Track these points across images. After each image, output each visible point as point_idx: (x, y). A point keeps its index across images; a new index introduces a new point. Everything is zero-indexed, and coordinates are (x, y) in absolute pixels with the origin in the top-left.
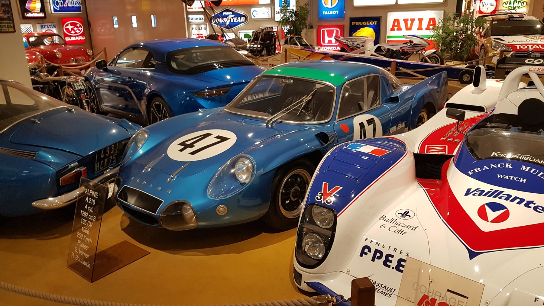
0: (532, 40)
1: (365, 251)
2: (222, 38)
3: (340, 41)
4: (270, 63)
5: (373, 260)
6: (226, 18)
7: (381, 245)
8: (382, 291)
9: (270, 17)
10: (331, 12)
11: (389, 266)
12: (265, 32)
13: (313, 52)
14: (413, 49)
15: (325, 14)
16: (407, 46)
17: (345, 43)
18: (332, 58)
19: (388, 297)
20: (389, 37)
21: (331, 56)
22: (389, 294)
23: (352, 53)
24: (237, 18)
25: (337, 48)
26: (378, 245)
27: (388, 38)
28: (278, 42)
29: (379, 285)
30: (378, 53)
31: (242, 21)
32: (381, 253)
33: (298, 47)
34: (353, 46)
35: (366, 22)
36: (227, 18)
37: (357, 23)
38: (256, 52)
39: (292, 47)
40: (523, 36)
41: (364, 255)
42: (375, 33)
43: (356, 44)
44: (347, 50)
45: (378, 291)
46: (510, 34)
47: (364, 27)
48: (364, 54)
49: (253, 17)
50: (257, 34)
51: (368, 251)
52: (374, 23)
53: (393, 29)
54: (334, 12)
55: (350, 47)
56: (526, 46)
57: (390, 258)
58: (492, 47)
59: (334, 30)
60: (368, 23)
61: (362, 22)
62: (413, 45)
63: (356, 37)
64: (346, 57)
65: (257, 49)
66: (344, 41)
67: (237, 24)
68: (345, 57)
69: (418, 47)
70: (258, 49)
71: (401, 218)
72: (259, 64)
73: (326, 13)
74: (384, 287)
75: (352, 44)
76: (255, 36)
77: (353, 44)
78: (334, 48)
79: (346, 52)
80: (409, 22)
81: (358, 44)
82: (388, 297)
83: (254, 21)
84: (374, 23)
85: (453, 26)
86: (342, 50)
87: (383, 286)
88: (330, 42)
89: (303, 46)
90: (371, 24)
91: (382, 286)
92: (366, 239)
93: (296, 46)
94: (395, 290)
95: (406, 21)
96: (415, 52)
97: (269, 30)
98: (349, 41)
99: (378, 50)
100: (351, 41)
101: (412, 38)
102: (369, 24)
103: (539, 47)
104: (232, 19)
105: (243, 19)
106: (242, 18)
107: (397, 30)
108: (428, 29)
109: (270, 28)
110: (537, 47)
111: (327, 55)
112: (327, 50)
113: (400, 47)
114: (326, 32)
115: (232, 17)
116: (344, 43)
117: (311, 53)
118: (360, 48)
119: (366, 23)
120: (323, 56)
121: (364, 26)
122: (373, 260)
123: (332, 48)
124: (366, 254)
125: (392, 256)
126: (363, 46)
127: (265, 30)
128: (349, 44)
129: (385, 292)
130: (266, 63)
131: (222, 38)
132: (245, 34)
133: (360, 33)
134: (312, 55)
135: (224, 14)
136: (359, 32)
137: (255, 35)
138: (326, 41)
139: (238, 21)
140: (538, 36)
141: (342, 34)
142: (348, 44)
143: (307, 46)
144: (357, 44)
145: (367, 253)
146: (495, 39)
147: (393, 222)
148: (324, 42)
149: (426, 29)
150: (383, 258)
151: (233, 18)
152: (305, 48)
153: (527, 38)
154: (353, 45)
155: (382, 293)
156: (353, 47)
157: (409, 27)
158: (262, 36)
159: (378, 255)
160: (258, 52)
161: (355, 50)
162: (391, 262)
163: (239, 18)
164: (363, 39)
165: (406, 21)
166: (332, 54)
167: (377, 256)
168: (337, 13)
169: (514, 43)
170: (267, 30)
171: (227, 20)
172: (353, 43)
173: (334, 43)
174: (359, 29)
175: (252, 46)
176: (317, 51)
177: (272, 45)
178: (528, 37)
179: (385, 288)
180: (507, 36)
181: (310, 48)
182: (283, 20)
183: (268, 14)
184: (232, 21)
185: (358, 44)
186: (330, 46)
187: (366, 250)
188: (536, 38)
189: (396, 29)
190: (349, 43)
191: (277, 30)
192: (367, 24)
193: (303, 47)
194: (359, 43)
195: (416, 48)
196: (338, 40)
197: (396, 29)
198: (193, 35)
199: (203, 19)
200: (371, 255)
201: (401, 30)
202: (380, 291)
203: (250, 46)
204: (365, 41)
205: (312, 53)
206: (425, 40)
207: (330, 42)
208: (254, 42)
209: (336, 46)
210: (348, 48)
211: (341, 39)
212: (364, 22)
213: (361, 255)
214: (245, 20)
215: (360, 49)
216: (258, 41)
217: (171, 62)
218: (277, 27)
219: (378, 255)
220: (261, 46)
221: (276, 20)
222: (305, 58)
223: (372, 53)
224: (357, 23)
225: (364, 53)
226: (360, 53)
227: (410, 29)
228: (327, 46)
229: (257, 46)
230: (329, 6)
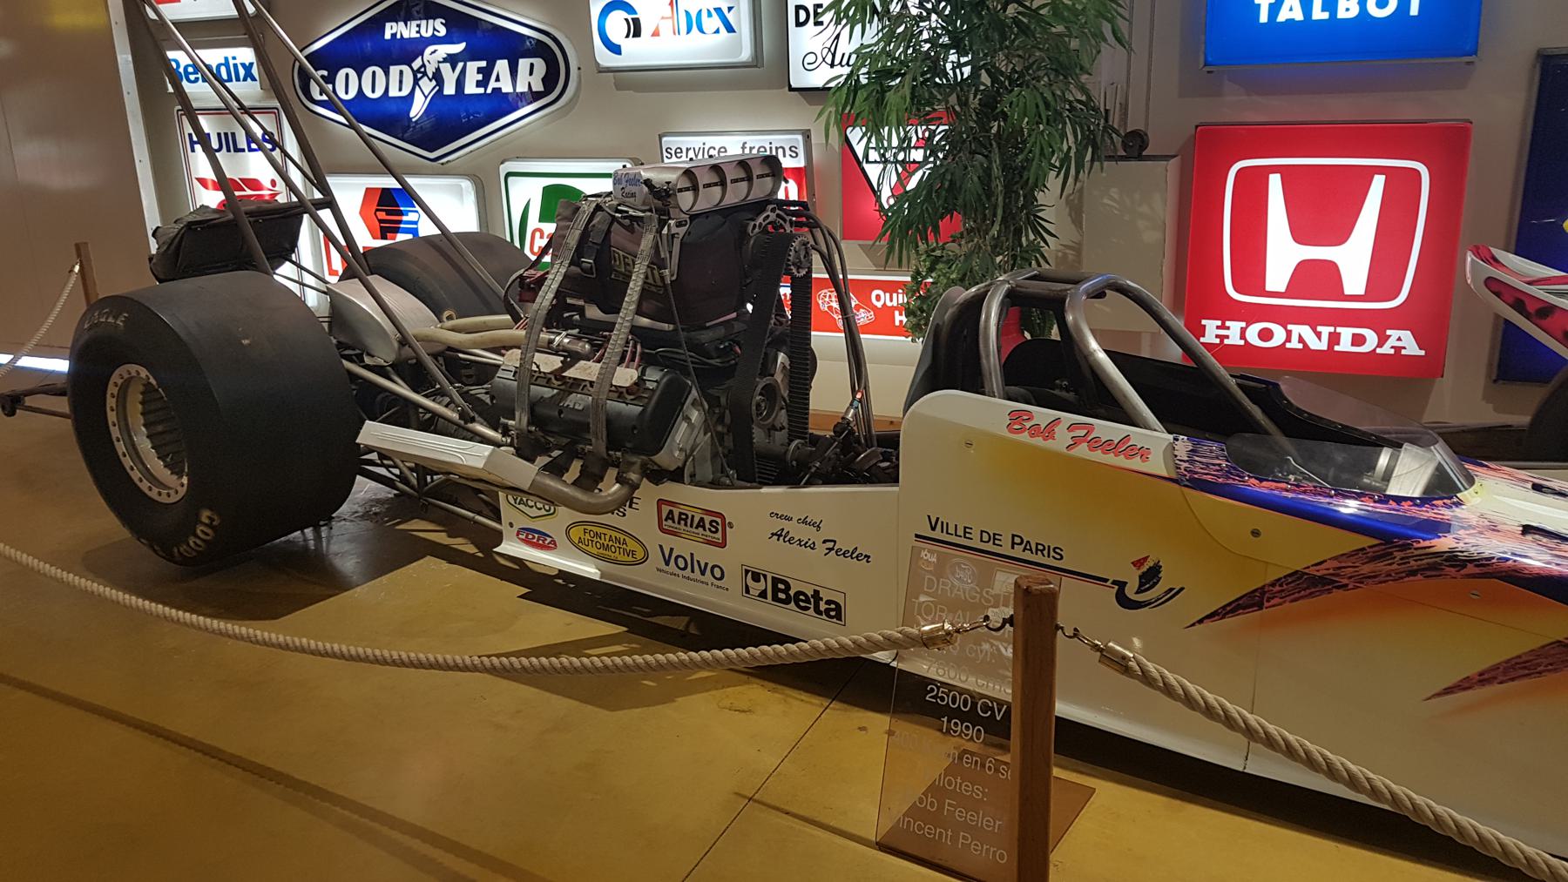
2: (382, 215)
4: (758, 564)
6: (405, 68)
9: (746, 54)
12: (693, 217)
15: (1282, 17)
24: (483, 64)
25: (1383, 340)
31: (522, 87)
33: (1122, 447)
36: (417, 64)
39: (1049, 431)
49: (605, 58)
59: (1370, 172)
67: (482, 110)
72: (632, 545)
83: (619, 86)
93: (1107, 429)
97: (736, 194)
104: (446, 68)
105: (530, 75)
106: (524, 64)
109: (743, 164)
115: (452, 60)
123: (1334, 339)
127: (686, 200)
130: (707, 554)
131: (382, 215)
132: (547, 191)
134: (1363, 579)
135: (388, 36)
137: (580, 251)
139: (497, 91)
151: (460, 65)
158: (657, 262)
163: (502, 66)
170: (710, 198)
171: (416, 82)
173: (1361, 291)
175: (547, 363)
177: (778, 344)
182: (880, 76)
183: (730, 29)
184: (449, 89)
191: (800, 162)
198: (197, 184)
199: (255, 71)
209: (1380, 323)
214: (550, 80)
218: (807, 135)
220: (653, 375)
221: (799, 78)
229: (608, 374)
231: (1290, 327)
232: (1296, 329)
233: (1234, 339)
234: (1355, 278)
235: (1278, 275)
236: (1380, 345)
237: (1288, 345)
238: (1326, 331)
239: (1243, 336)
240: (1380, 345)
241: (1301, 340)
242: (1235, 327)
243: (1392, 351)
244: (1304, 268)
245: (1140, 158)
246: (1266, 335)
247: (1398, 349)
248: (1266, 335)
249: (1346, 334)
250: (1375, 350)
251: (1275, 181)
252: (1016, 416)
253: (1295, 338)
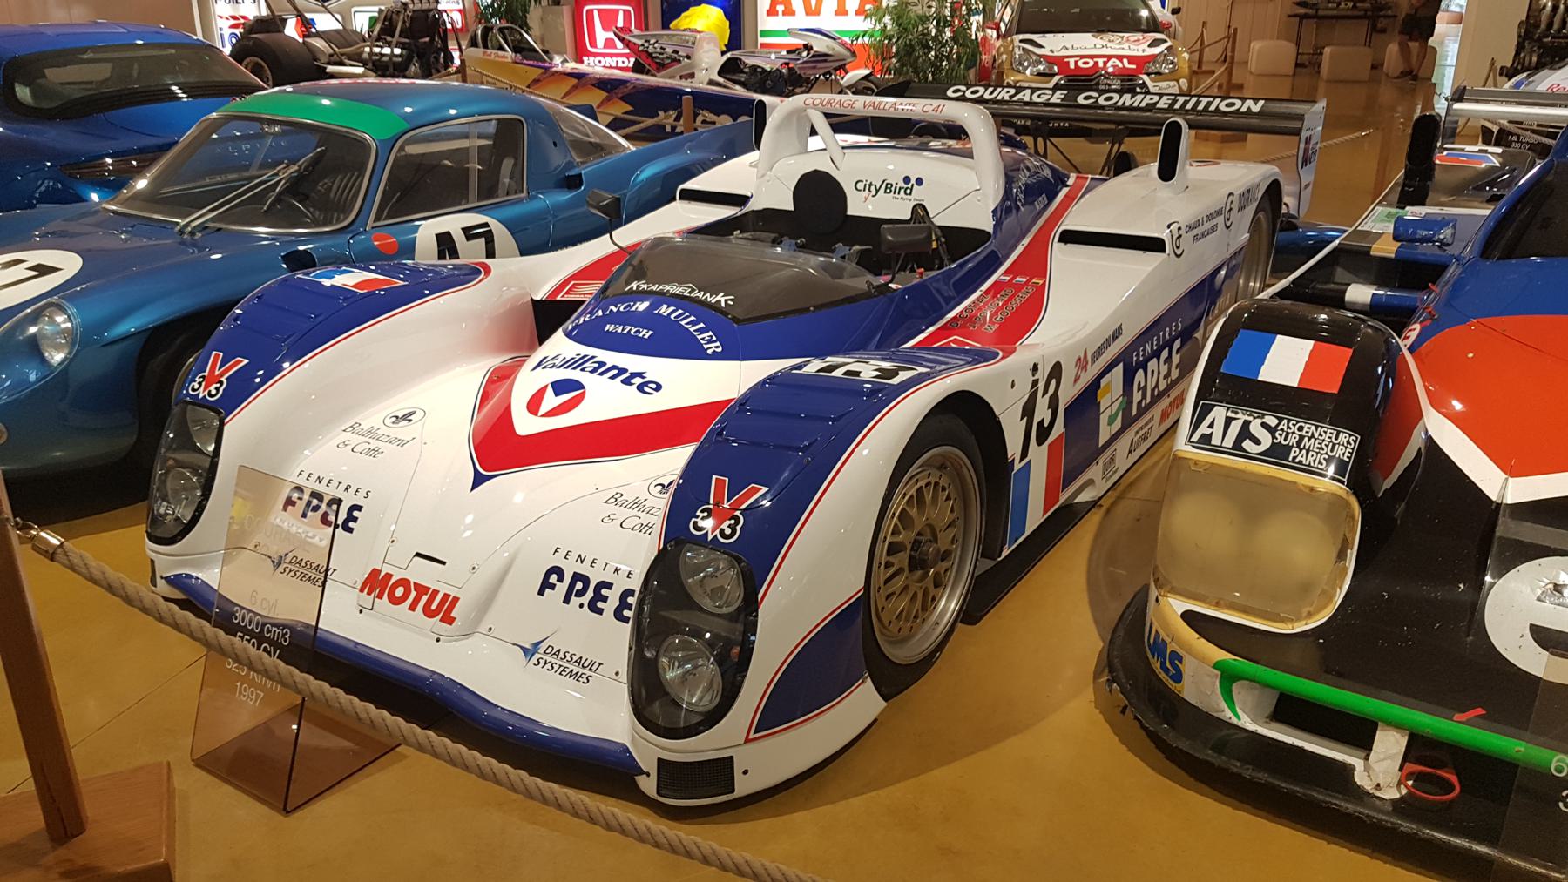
0: (1109, 45)
1: (551, 581)
3: (630, 41)
5: (567, 600)
7: (588, 562)
8: (572, 671)
11: (600, 611)
13: (546, 69)
16: (798, 59)
17: (641, 48)
18: (599, 88)
19: (584, 683)
20: (765, 33)
21: (594, 82)
22: (585, 677)
23: (662, 77)
26: (582, 562)
27: (761, 36)
28: (455, 42)
29: (565, 657)
30: (729, 76)
32: (586, 580)
33: (504, 57)
34: (661, 56)
38: (391, 70)
39: (490, 55)
40: (1090, 34)
41: (547, 591)
42: (728, 23)
43: (669, 50)
44: (648, 67)
45: (563, 670)
46: (1054, 29)
48: (693, 80)
50: (391, 16)
51: (558, 580)
53: (772, 12)
55: (656, 57)
56: (1092, 59)
57: (604, 592)
58: (1012, 65)
59: (618, 10)
63: (679, 30)
64: (634, 87)
65: (390, 59)
66: (639, 42)
68: (632, 86)
70: (395, 59)
71: (659, 495)
74: (576, 661)
75: (658, 50)
76: (386, 23)
77: (662, 51)
78: (623, 62)
79: (648, 73)
81: (676, 52)
82: (584, 683)
85: (920, 7)
86: (638, 68)
87: (575, 658)
89: (520, 53)
91: (572, 659)
92: (556, 551)
93: (500, 53)
94: (600, 664)
96: (822, 77)
98: (652, 41)
99: (730, 69)
100: (661, 42)
101: (812, 36)
103: (1122, 63)
107: (784, 13)
110: (1118, 63)
111: (583, 81)
112: (604, 66)
113: (784, 61)
114: (596, 13)
117: (542, 73)
120: (575, 81)
122: (567, 600)
124: (552, 587)
125: (609, 586)
126: (688, 57)
128: (651, 49)
129: (577, 673)
133: (688, 20)
134: (544, 79)
136: (686, 17)
138: (600, 42)
140: (1126, 35)
141: (643, 24)
142: (650, 51)
143: (530, 54)
144: (672, 51)
145: (555, 585)
146: (1021, 41)
147: (636, 505)
148: (593, 44)
149: (858, 13)
150: (590, 594)
152: (524, 58)
153: (1098, 41)
154: (662, 54)
155: (570, 677)
156: (663, 59)
157: (813, 7)
159: (579, 585)
160: (394, 70)
161: (668, 68)
162: (605, 599)
164: (687, 38)
166: (598, 77)
167: (577, 590)
169: (1064, 53)
172: (662, 48)
174: (687, 10)
176: (560, 68)
178: (1101, 38)
179: (579, 663)
180: (1052, 35)
181: (545, 61)
185: (676, 52)
186: (611, 55)
187: (553, 578)
188: (1120, 40)
189: (780, 13)
190: (651, 47)
193: (518, 55)
194: (677, 48)
196: (624, 39)
197: (780, 13)
200: (562, 588)
201: (793, 13)
202: (568, 670)
203: (371, 49)
204: (694, 43)
205: (545, 73)
206: (843, 44)
207: (609, 43)
208: (385, 39)
210: (650, 60)
211: (634, 36)
213: (541, 592)
215: (680, 65)
216: (393, 37)
217: (16, 85)
219: (579, 585)
222: (524, 88)
223: (712, 77)
225: (692, 76)
226: (681, 77)
227: (817, 12)
228: (604, 55)
252: (484, 53)
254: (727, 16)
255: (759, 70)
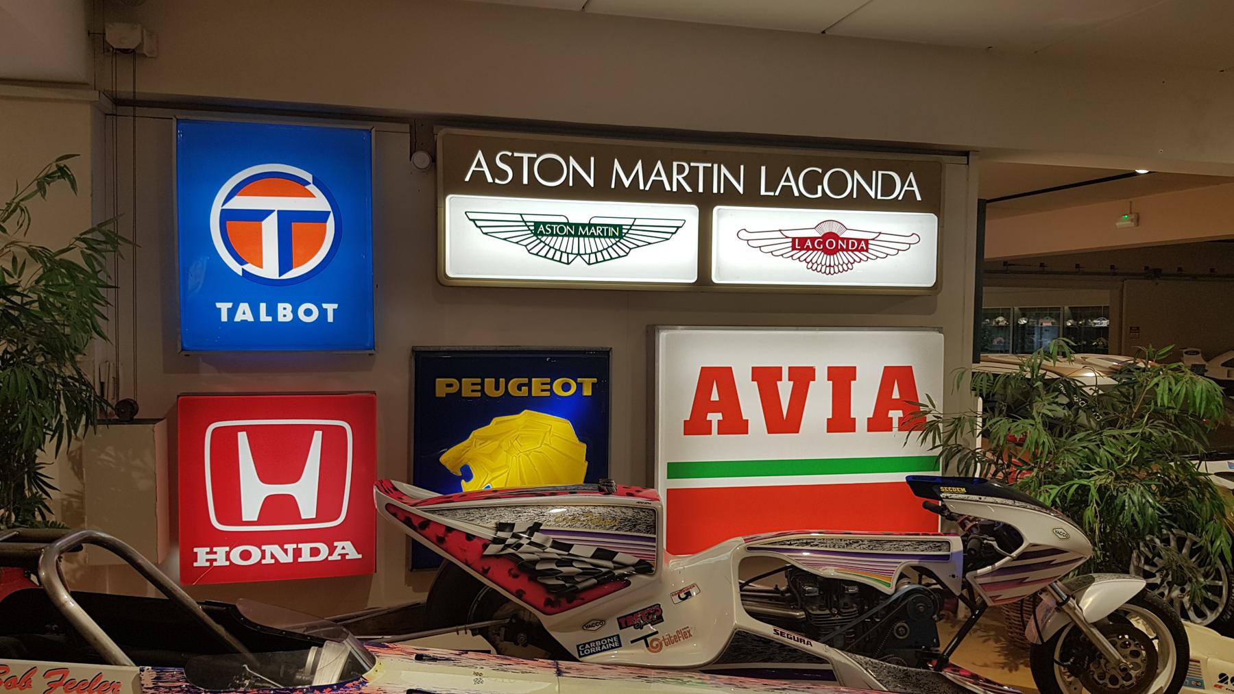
3: (449, 529)
10: (285, 312)
14: (1021, 582)
17: (493, 549)
25: (332, 550)
34: (564, 569)
35: (525, 380)
37: (468, 387)
43: (582, 550)
47: (517, 412)
52: (580, 386)
53: (696, 426)
54: (308, 313)
55: (546, 573)
60: (538, 387)
61: (502, 380)
62: (1023, 556)
69: (1048, 565)
73: (244, 313)
75: (553, 553)
80: (785, 388)
84: (580, 386)
88: (278, 508)
90: (559, 392)
95: (766, 378)
102: (547, 394)
108: (878, 423)
116: (485, 546)
118: (623, 582)
119: (529, 385)
121: (512, 406)
123: (297, 553)
136: (486, 439)
144: (592, 551)
154: (569, 563)
156: (569, 578)
165: (766, 378)
168: (330, 319)
172: (556, 545)
185: (601, 554)
192: (534, 394)
194: (608, 544)
195: (1032, 575)
207: (278, 508)
209: (329, 537)
212: (514, 382)
224: (468, 387)
230: (269, 268)
231: (264, 547)
232: (268, 549)
233: (221, 561)
234: (308, 508)
235: (251, 508)
236: (331, 554)
237: (264, 562)
238: (290, 547)
239: (228, 558)
240: (331, 554)
241: (273, 556)
242: (221, 551)
243: (339, 558)
244: (270, 501)
245: (132, 421)
246: (246, 555)
247: (343, 556)
248: (246, 555)
249: (306, 548)
250: (327, 558)
251: (242, 437)
253: (268, 555)
254: (582, 434)
255: (853, 590)
